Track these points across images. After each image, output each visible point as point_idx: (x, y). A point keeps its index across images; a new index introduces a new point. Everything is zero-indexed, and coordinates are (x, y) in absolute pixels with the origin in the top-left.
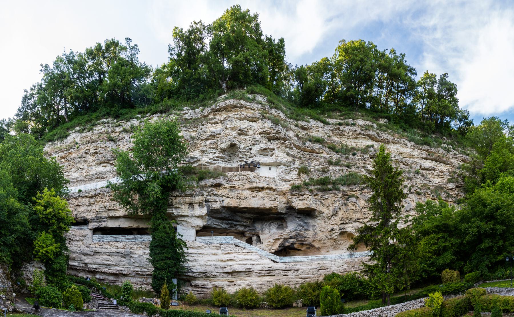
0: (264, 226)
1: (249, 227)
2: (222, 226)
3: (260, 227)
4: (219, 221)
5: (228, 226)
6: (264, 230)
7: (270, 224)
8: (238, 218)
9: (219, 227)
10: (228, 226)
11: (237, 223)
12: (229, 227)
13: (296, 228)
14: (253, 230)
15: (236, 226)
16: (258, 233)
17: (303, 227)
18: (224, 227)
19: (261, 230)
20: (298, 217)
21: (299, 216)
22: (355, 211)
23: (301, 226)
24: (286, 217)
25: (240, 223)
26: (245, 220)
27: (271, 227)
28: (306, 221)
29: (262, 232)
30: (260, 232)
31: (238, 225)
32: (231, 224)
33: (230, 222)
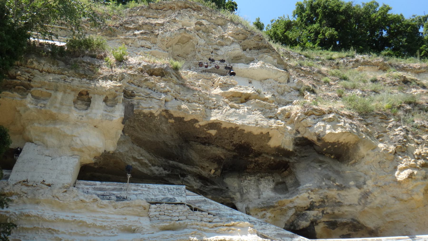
0: (245, 183)
1: (213, 183)
2: (153, 168)
3: (236, 185)
4: (147, 155)
5: (166, 172)
6: (245, 191)
7: (259, 180)
8: (193, 155)
9: (145, 171)
10: (166, 172)
12: (168, 175)
13: (321, 183)
14: (221, 190)
17: (334, 181)
18: (157, 173)
23: (329, 179)
24: (293, 163)
25: (194, 170)
26: (206, 164)
27: (261, 187)
28: (336, 168)
29: (242, 195)
30: (238, 195)
31: (190, 173)
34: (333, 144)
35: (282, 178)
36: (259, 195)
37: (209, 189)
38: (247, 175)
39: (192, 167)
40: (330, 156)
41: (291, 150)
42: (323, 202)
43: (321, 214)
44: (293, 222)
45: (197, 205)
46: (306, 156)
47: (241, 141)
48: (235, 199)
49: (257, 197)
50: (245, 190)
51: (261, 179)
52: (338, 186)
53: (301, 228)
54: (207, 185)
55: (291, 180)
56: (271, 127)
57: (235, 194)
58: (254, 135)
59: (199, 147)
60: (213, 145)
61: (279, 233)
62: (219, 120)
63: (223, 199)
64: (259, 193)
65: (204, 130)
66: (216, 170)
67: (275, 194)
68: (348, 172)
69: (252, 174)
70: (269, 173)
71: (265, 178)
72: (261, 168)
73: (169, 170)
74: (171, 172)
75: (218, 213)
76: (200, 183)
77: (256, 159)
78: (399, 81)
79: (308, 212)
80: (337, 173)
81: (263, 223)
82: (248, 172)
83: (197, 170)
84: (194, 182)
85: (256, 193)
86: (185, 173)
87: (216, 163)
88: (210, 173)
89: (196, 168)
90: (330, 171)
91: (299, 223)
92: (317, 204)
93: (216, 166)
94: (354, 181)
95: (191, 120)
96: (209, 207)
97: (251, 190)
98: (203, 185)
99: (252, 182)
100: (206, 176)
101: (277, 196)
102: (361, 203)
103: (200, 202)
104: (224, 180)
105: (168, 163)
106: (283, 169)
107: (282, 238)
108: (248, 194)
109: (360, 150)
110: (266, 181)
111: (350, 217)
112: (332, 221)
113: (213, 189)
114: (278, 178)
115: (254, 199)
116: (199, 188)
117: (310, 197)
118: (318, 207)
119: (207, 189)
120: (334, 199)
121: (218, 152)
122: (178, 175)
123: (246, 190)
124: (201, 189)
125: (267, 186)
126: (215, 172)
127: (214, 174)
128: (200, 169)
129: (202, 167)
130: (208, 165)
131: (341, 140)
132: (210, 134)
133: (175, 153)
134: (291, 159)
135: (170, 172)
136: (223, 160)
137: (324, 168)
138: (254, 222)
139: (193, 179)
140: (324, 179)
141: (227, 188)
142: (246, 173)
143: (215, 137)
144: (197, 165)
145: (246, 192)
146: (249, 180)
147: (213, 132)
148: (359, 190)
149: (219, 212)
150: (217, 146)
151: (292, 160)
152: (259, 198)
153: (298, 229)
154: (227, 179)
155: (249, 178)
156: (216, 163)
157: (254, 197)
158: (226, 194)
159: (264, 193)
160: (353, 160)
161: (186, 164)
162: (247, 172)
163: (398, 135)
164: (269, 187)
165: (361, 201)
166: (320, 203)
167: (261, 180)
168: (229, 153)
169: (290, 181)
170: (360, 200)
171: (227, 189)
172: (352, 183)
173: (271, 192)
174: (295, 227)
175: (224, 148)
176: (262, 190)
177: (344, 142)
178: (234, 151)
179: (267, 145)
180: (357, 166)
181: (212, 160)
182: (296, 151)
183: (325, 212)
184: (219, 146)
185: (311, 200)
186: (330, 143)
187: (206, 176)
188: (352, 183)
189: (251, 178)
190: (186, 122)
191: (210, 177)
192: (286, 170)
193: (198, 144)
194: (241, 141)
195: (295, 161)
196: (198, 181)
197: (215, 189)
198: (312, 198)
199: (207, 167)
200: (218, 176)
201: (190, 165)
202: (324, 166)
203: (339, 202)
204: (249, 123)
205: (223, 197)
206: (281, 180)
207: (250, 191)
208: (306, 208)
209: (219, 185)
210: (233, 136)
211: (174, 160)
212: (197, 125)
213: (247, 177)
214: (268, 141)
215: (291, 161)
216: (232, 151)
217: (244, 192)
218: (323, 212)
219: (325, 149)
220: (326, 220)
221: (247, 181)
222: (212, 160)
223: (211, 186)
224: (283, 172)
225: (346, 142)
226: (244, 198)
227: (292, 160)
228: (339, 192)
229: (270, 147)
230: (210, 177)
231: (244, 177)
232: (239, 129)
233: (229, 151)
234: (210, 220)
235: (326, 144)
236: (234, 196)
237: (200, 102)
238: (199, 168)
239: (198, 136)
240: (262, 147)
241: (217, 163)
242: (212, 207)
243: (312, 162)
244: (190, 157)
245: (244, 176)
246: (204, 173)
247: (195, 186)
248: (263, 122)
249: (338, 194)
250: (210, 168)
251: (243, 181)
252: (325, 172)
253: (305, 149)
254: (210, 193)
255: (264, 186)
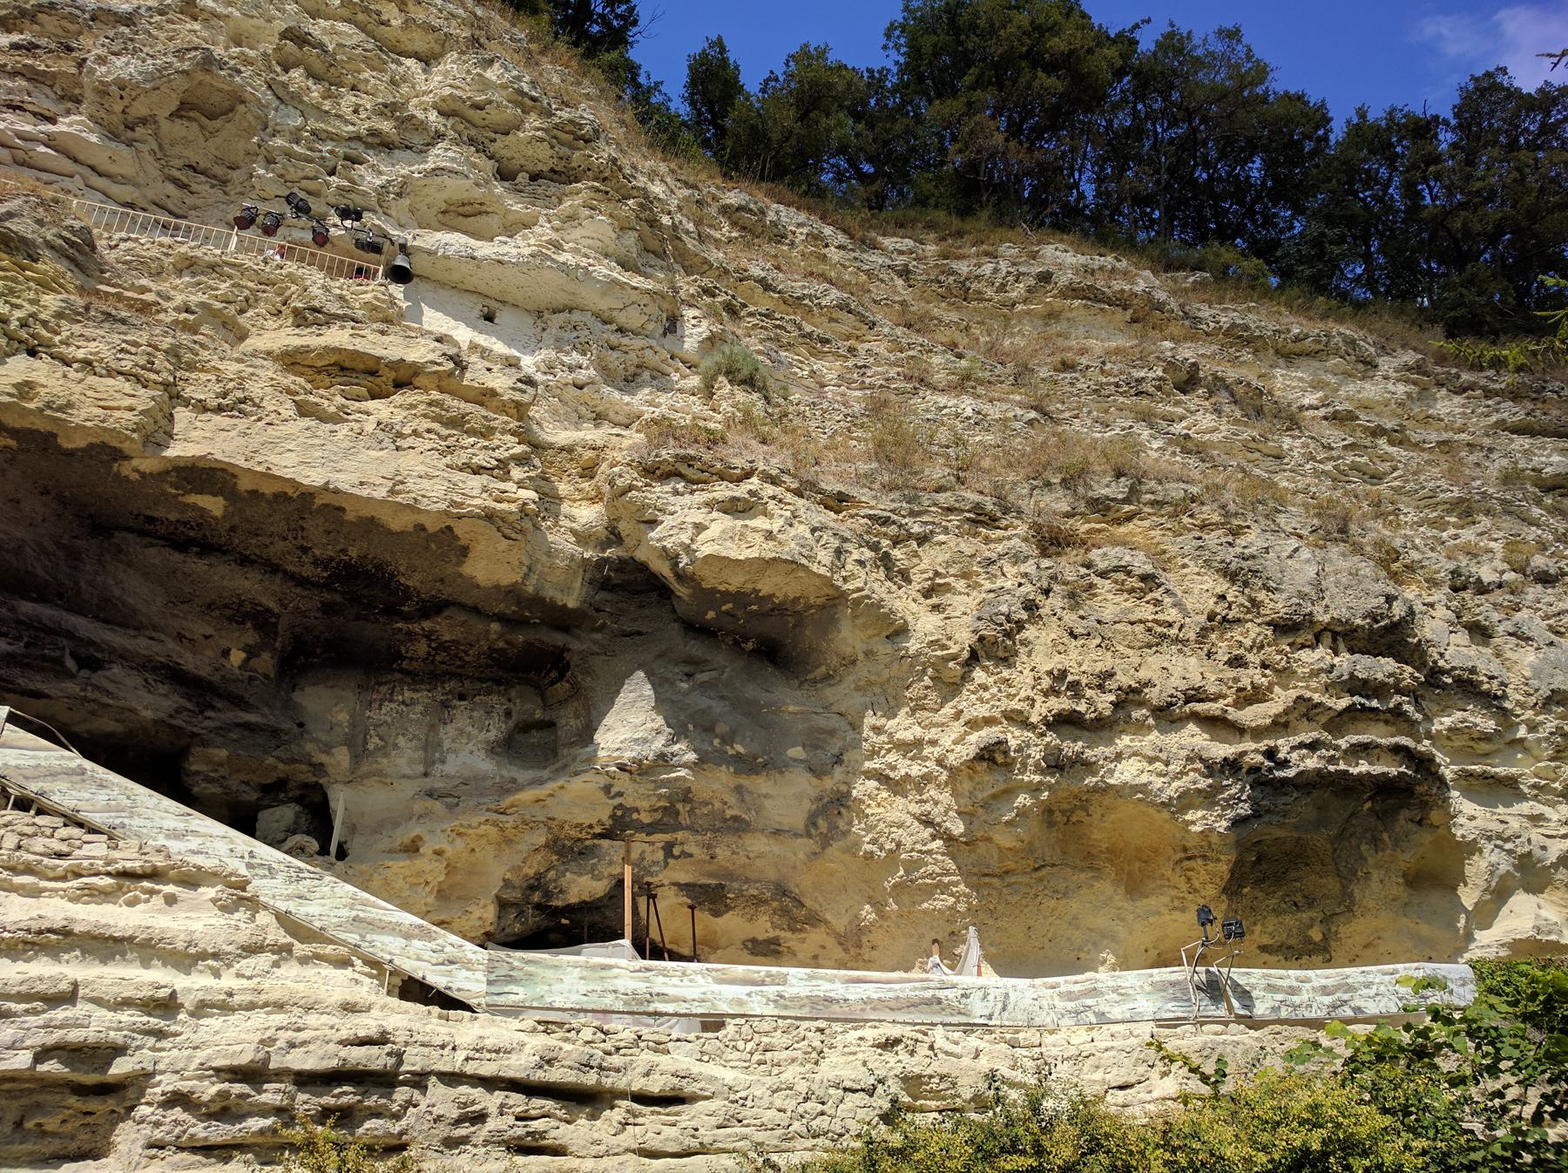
0: (387, 712)
1: (239, 702)
3: (343, 717)
6: (374, 742)
7: (445, 705)
8: (134, 590)
11: (114, 638)
14: (275, 732)
15: (91, 663)
16: (319, 768)
19: (349, 742)
20: (690, 661)
21: (696, 648)
22: (1159, 637)
25: (141, 645)
26: (200, 627)
27: (447, 733)
28: (751, 691)
29: (359, 754)
30: (342, 757)
31: (124, 657)
32: (37, 631)
33: (27, 607)
34: (740, 598)
35: (546, 706)
36: (429, 763)
37: (217, 724)
38: (402, 682)
39: (132, 632)
40: (736, 643)
41: (572, 603)
42: (670, 811)
43: (660, 855)
44: (539, 876)
45: (33, 787)
46: (640, 634)
47: (344, 551)
48: (330, 770)
49: (421, 769)
50: (377, 740)
51: (456, 702)
52: (738, 758)
53: (573, 900)
54: (213, 708)
55: (577, 717)
56: (460, 505)
57: (328, 753)
58: (390, 533)
59: (158, 556)
60: (224, 553)
61: (362, 915)
62: (219, 456)
63: (281, 766)
64: (431, 751)
65: (164, 493)
66: (251, 652)
67: (498, 764)
68: (791, 708)
69: (422, 682)
70: (498, 682)
71: (477, 699)
72: (461, 659)
73: (18, 638)
74: (27, 645)
75: (117, 821)
76: (176, 697)
77: (427, 625)
78: (1160, 379)
79: (605, 843)
80: (752, 712)
81: (306, 875)
82: (408, 673)
83: (156, 647)
84: (143, 693)
85: (420, 754)
86: (99, 655)
87: (249, 625)
88: (223, 661)
89: (152, 638)
90: (722, 698)
91: (563, 882)
92: (646, 818)
93: (251, 637)
94: (804, 746)
95: (92, 446)
96: (87, 796)
97: (401, 741)
98: (189, 705)
99: (415, 713)
100: (204, 672)
101: (504, 772)
102: (813, 831)
103: (53, 774)
104: (297, 696)
105: (12, 609)
106: (554, 674)
107: (368, 937)
108: (386, 755)
109: (839, 631)
110: (475, 714)
111: (772, 875)
112: (709, 886)
113: (238, 725)
114: (528, 706)
115: (404, 776)
116: (162, 715)
117: (614, 790)
118: (651, 829)
119: (207, 723)
120: (718, 805)
121: (247, 583)
122: (59, 661)
123: (381, 739)
124: (178, 722)
125: (475, 732)
126: (246, 661)
127: (244, 665)
128: (171, 645)
129: (180, 637)
130: (210, 631)
131: (765, 587)
132: (202, 511)
133: (40, 572)
134: (578, 638)
135: (19, 648)
136: (278, 616)
137: (702, 685)
138: (270, 869)
139: (140, 681)
140: (691, 727)
141: (301, 725)
142: (397, 676)
143: (227, 526)
144: (155, 628)
145: (377, 749)
146: (403, 702)
147: (214, 505)
148: (814, 781)
149: (126, 821)
150: (245, 561)
151: (577, 645)
152: (426, 775)
153: (560, 903)
154: (309, 690)
155: (407, 694)
156: (249, 625)
157: (407, 771)
158: (294, 748)
159: (451, 758)
160: (819, 666)
161: (106, 621)
162: (401, 671)
163: (1009, 592)
164: (482, 736)
165: (815, 825)
166: (658, 816)
167: (455, 707)
168: (298, 590)
169: (572, 722)
170: (812, 821)
171: (296, 729)
172: (796, 752)
173: (483, 755)
174: (548, 894)
175: (273, 568)
176: (446, 744)
177: (780, 596)
178: (327, 586)
179: (461, 575)
180: (828, 691)
181: (228, 612)
182: (598, 610)
183: (676, 851)
184: (254, 562)
185: (618, 801)
186: (727, 596)
187: (203, 673)
188: (796, 752)
189: (415, 696)
190: (70, 453)
191: (223, 677)
192: (561, 678)
193: (152, 545)
194: (344, 551)
195: (595, 649)
196: (163, 689)
197: (247, 726)
198: (620, 794)
199: (206, 637)
200: (267, 677)
201: (126, 626)
202: (702, 677)
203: (736, 819)
204: (362, 483)
205: (279, 759)
206: (538, 715)
207: (396, 746)
208: (598, 830)
209: (266, 710)
210: (303, 529)
211: (42, 598)
212: (126, 469)
213: (398, 689)
214: (460, 563)
215: (576, 645)
216: (315, 585)
217: (371, 747)
218: (668, 848)
219: (711, 615)
220: (684, 878)
221: (393, 706)
222: (228, 612)
223: (230, 715)
224: (552, 683)
225: (792, 596)
226: (364, 768)
227: (577, 645)
228: (744, 781)
229: (478, 586)
230: (223, 677)
231: (384, 689)
232: (318, 502)
233: (303, 582)
234: (64, 848)
235: (711, 597)
236: (323, 758)
237: (153, 376)
238: (163, 637)
239: (149, 513)
240: (442, 580)
241: (256, 627)
242: (102, 797)
243: (659, 656)
244: (117, 593)
245: (380, 684)
246: (190, 661)
247: (146, 708)
248: (426, 484)
249: (739, 790)
250: (224, 643)
251: (375, 705)
252: (702, 701)
253: (641, 607)
254: (219, 740)
255: (461, 732)
